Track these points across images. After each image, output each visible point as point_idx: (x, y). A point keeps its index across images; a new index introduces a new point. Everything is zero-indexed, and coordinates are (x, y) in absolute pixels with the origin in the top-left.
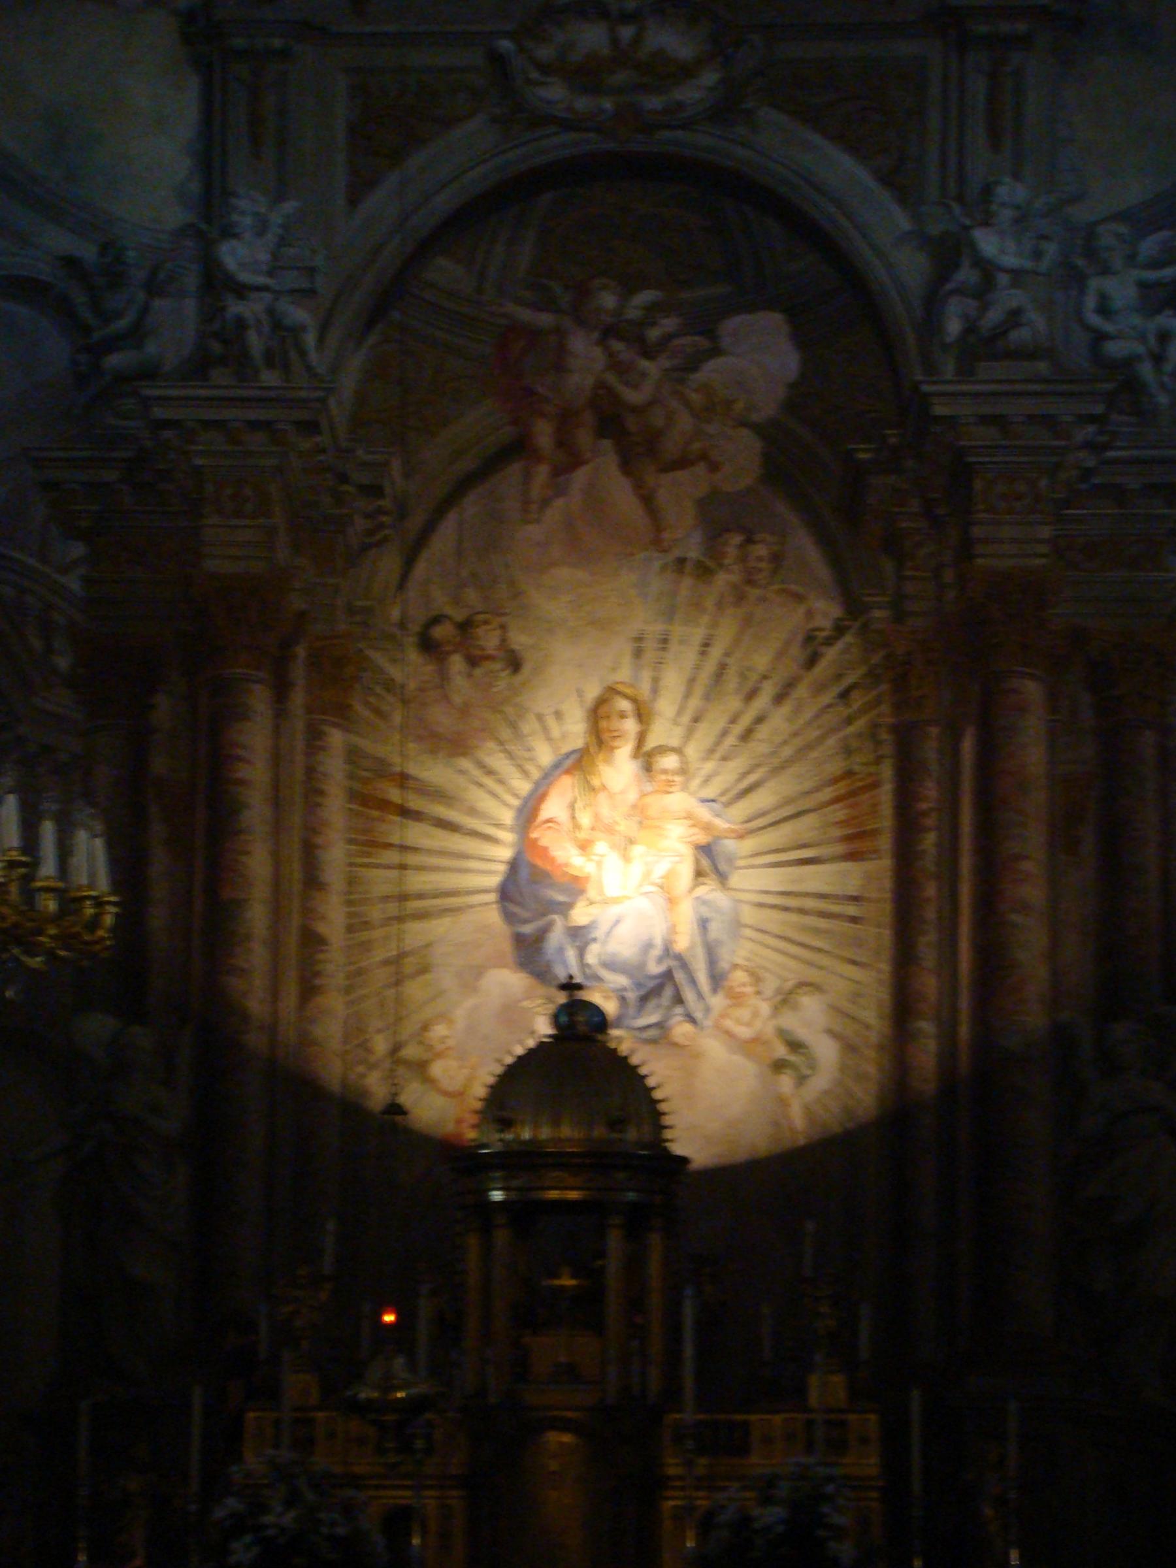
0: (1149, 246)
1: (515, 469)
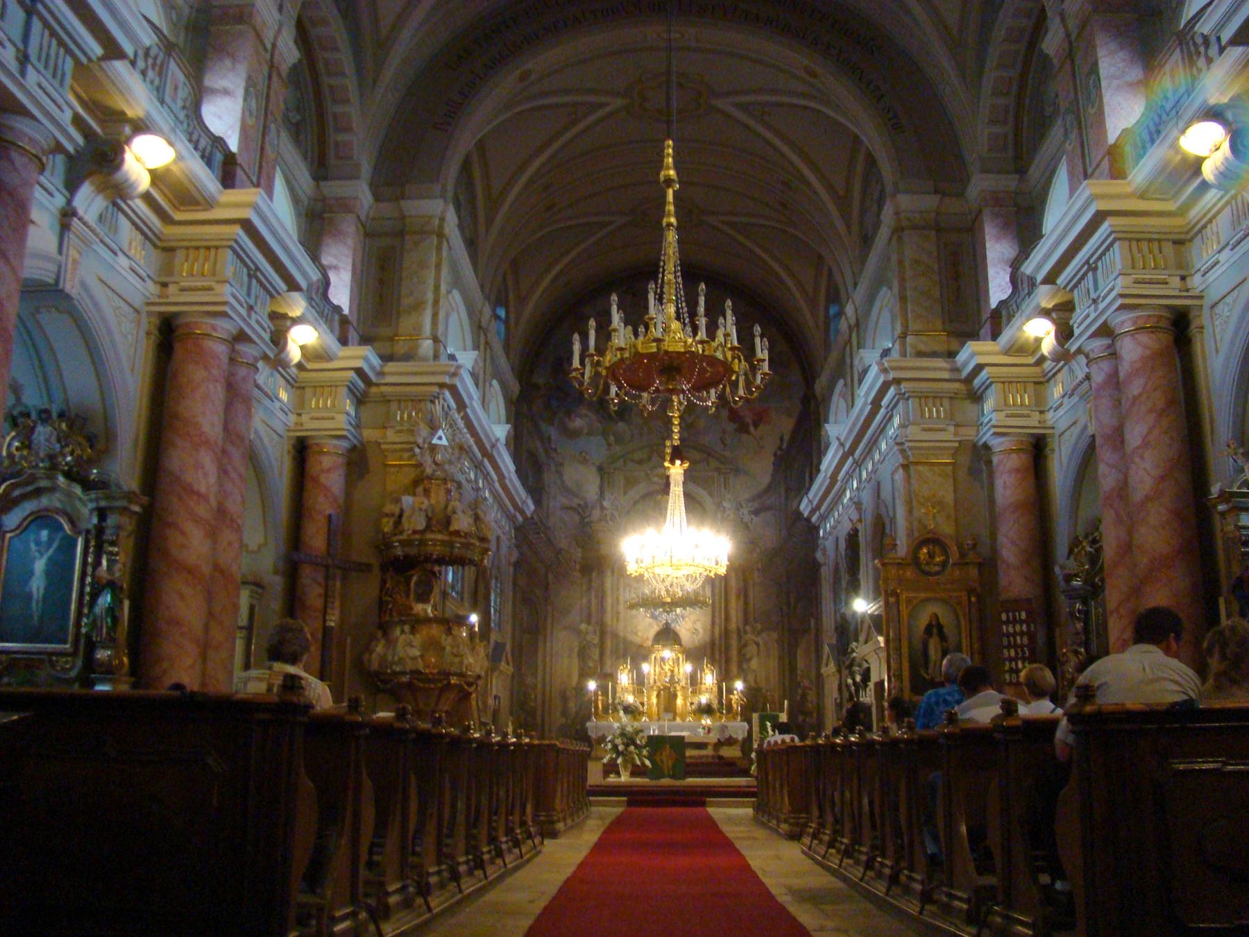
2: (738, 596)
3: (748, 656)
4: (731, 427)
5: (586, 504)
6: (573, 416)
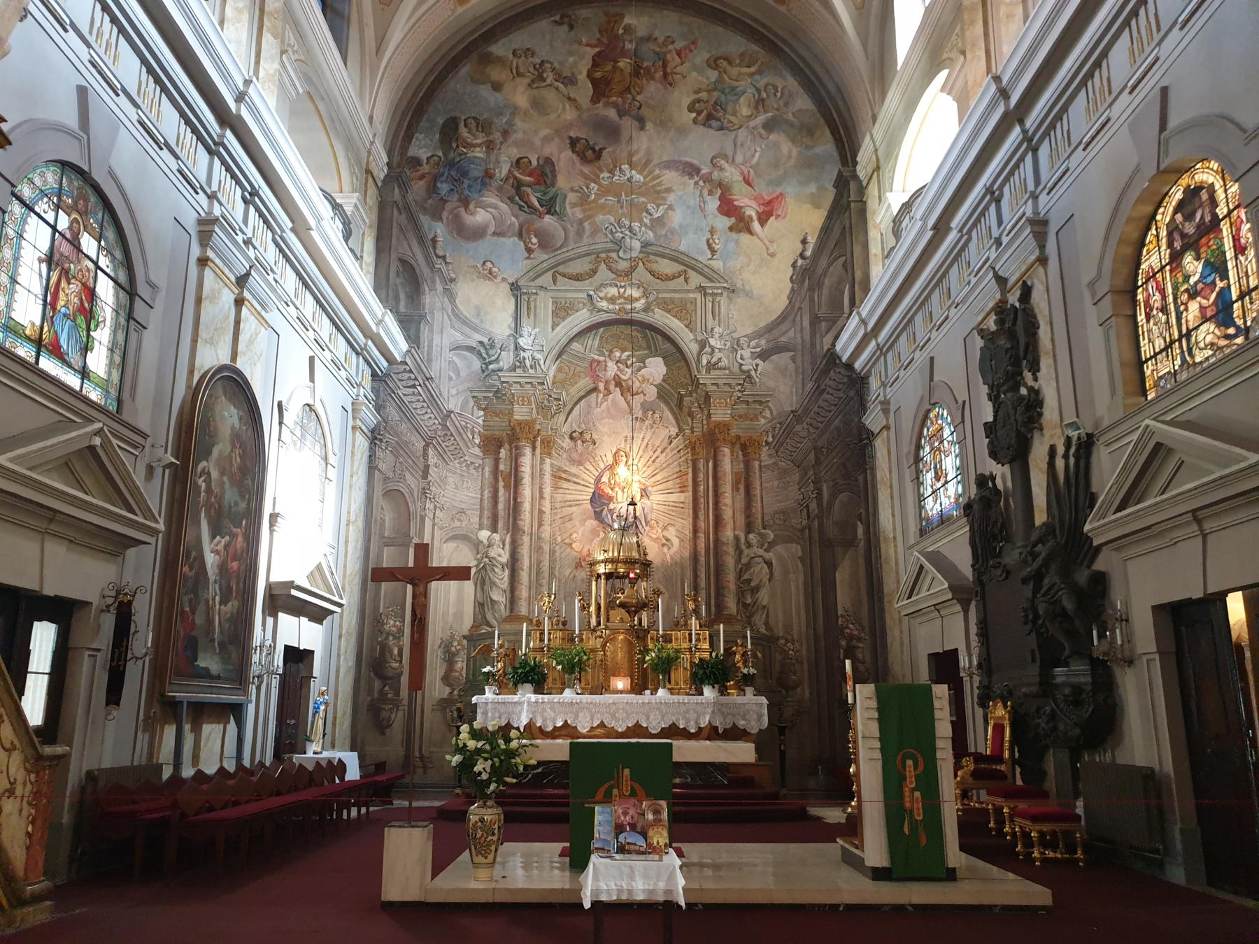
0: (753, 343)
1: (594, 395)
2: (735, 488)
3: (753, 584)
4: (724, 222)
5: (492, 346)
6: (471, 206)
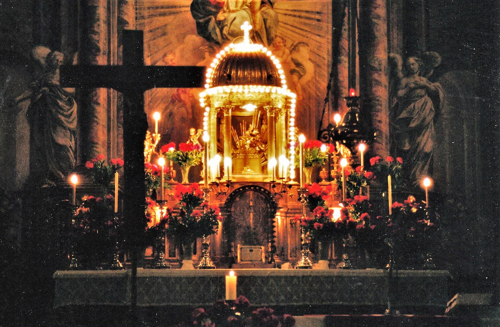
3: (413, 125)
